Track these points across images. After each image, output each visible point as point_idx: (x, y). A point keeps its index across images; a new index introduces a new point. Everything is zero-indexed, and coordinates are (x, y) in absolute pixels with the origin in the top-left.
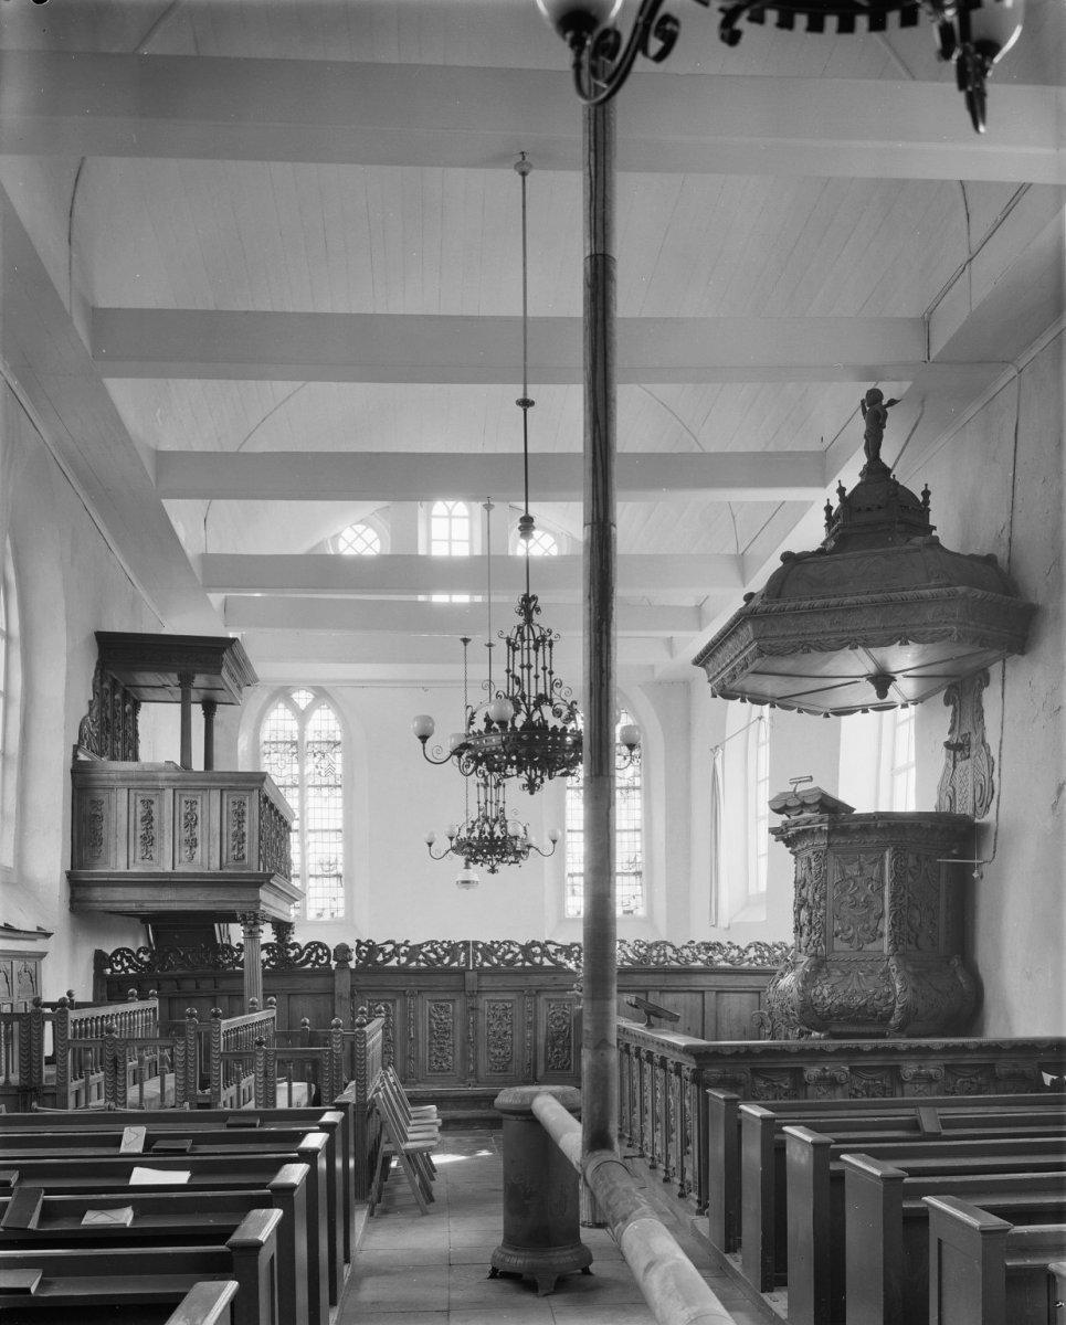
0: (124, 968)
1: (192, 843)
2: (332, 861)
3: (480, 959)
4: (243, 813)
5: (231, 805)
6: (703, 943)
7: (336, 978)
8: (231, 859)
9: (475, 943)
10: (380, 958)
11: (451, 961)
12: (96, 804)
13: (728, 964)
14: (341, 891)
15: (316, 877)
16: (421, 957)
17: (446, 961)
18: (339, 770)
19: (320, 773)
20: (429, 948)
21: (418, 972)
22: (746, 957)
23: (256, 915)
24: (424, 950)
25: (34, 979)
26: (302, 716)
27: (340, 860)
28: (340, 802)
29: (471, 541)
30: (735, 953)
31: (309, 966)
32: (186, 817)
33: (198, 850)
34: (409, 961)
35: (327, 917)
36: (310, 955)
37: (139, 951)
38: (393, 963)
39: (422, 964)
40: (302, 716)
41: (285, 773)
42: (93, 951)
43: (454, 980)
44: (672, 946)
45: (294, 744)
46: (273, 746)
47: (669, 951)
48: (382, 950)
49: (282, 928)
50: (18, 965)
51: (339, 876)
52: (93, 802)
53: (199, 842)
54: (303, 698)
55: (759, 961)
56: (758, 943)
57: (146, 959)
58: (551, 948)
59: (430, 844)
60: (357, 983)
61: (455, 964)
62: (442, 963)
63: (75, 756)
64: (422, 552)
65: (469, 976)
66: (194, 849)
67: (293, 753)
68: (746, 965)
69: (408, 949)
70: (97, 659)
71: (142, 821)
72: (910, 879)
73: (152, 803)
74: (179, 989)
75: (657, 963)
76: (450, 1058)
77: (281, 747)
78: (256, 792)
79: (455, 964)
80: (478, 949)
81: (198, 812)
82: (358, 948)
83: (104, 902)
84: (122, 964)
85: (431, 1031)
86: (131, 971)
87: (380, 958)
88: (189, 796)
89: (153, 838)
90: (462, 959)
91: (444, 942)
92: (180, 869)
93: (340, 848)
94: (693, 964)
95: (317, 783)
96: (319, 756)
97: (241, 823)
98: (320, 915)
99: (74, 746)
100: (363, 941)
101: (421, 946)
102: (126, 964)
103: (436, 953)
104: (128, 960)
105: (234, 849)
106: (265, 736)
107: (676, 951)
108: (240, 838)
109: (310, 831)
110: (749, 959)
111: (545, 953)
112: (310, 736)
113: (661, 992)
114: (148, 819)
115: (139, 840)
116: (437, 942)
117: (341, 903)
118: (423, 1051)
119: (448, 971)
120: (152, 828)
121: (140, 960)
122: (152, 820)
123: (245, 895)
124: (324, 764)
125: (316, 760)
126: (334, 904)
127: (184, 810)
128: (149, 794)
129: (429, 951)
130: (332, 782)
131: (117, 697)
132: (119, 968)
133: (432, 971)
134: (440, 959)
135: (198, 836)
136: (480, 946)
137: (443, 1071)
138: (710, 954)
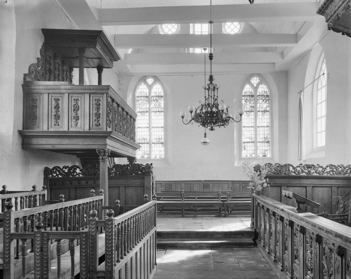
0: (57, 175)
1: (77, 118)
2: (160, 138)
4: (99, 105)
5: (94, 101)
6: (306, 165)
7: (145, 179)
8: (94, 125)
12: (35, 100)
13: (317, 174)
14: (163, 149)
15: (155, 143)
18: (162, 106)
19: (156, 107)
22: (325, 171)
23: (105, 151)
26: (150, 87)
27: (163, 137)
28: (163, 117)
30: (320, 169)
32: (74, 107)
33: (79, 121)
35: (158, 157)
37: (63, 167)
40: (150, 87)
41: (144, 107)
42: (44, 168)
44: (292, 166)
45: (147, 97)
46: (140, 98)
47: (291, 168)
49: (131, 159)
51: (162, 143)
52: (33, 100)
53: (80, 118)
54: (150, 81)
55: (331, 173)
56: (331, 165)
57: (66, 171)
59: (183, 117)
63: (25, 79)
64: (191, 32)
66: (77, 121)
67: (147, 100)
68: (325, 174)
70: (43, 41)
73: (59, 100)
75: (285, 174)
77: (143, 98)
78: (105, 95)
81: (79, 104)
83: (37, 145)
84: (56, 173)
86: (60, 176)
88: (75, 97)
89: (59, 116)
92: (71, 130)
93: (163, 133)
94: (302, 174)
95: (155, 111)
96: (156, 101)
97: (98, 109)
98: (156, 157)
99: (25, 75)
102: (58, 173)
104: (59, 171)
106: (137, 94)
107: (294, 168)
108: (98, 116)
109: (152, 127)
110: (327, 172)
112: (153, 94)
113: (288, 186)
114: (57, 107)
115: (53, 117)
117: (163, 153)
120: (59, 111)
121: (64, 171)
122: (59, 108)
123: (100, 142)
124: (157, 104)
125: (155, 102)
126: (161, 153)
127: (73, 103)
128: (58, 96)
130: (160, 110)
131: (65, 68)
132: (55, 175)
135: (79, 115)
138: (309, 170)
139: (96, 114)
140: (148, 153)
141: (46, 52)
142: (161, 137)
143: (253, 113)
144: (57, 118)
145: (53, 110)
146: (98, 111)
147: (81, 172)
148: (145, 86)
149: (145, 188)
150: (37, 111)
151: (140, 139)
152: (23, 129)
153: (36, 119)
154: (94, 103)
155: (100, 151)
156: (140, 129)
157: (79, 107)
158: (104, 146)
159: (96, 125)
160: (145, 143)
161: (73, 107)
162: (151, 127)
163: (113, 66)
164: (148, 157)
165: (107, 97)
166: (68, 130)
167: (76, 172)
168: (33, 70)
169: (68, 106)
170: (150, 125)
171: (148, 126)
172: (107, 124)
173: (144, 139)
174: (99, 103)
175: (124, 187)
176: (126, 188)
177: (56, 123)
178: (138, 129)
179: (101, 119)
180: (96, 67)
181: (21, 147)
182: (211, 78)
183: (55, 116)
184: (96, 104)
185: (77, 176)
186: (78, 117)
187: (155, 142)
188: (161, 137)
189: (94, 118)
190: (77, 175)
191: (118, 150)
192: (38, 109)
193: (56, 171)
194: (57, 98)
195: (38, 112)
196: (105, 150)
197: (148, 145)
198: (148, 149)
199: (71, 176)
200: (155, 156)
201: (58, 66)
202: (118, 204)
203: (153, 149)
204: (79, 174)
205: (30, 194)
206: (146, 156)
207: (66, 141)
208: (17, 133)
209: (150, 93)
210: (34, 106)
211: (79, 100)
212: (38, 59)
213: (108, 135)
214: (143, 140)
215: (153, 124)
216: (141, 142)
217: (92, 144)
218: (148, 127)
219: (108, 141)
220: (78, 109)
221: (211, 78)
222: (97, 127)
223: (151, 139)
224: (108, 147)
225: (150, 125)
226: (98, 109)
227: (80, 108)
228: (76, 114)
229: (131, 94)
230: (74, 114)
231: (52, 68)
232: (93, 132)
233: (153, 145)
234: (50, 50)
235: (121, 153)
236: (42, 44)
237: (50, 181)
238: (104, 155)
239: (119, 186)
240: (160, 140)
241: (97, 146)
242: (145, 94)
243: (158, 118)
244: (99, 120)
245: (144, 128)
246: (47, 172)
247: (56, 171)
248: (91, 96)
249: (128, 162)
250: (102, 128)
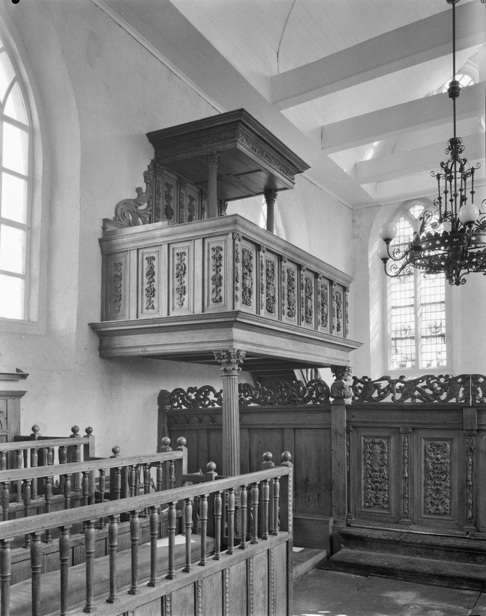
1: (182, 291)
3: (481, 395)
4: (220, 258)
5: (211, 251)
7: (333, 414)
8: (211, 302)
9: (476, 377)
10: (375, 395)
11: (450, 397)
12: (118, 265)
14: (444, 347)
15: (427, 337)
16: (417, 393)
17: (444, 397)
20: (424, 384)
21: (413, 409)
23: (229, 354)
24: (419, 386)
27: (444, 324)
31: (310, 403)
32: (177, 269)
33: (186, 297)
34: (405, 396)
35: (434, 365)
36: (311, 393)
38: (388, 399)
39: (418, 401)
42: (158, 391)
48: (377, 387)
51: (442, 336)
53: (186, 290)
57: (193, 397)
60: (353, 419)
61: (453, 400)
62: (439, 399)
63: (104, 228)
65: (467, 412)
66: (183, 296)
69: (403, 385)
70: (152, 156)
71: (147, 275)
73: (154, 258)
74: (213, 422)
76: (448, 501)
78: (230, 236)
79: (453, 400)
80: (478, 384)
81: (186, 262)
82: (355, 384)
83: (120, 348)
84: (178, 402)
85: (426, 468)
86: (184, 407)
87: (375, 395)
89: (154, 290)
90: (461, 395)
91: (441, 376)
92: (172, 314)
93: (443, 315)
97: (218, 267)
98: (429, 365)
99: (105, 221)
100: (359, 377)
101: (416, 382)
103: (432, 389)
104: (182, 398)
105: (213, 291)
108: (218, 281)
109: (422, 304)
114: (151, 273)
115: (145, 292)
116: (433, 377)
117: (444, 356)
118: (419, 492)
119: (445, 408)
120: (154, 281)
121: (189, 398)
122: (154, 274)
126: (439, 356)
127: (176, 262)
128: (151, 252)
129: (425, 387)
133: (429, 407)
134: (436, 395)
135: (185, 284)
136: (481, 380)
137: (439, 514)
139: (214, 279)
140: (414, 357)
141: (156, 177)
142: (441, 324)
144: (151, 294)
145: (146, 280)
146: (217, 272)
147: (216, 399)
148: (407, 223)
149: (333, 433)
150: (121, 286)
151: (396, 331)
152: (102, 320)
153: (120, 299)
154: (211, 255)
155: (220, 354)
156: (398, 310)
157: (185, 268)
158: (227, 344)
159: (214, 302)
160: (406, 338)
161: (175, 269)
162: (418, 304)
163: (294, 184)
164: (413, 366)
165: (234, 240)
166: (168, 314)
167: (208, 399)
168: (123, 211)
169: (167, 269)
170: (416, 301)
171: (412, 303)
172: (234, 298)
173: (406, 330)
174: (220, 255)
175: (292, 431)
176: (297, 432)
177: (150, 305)
178: (393, 311)
179: (222, 288)
180: (263, 191)
181: (98, 354)
183: (148, 291)
184: (214, 258)
185: (210, 406)
186: (185, 287)
187: (428, 334)
188: (441, 324)
189: (212, 287)
190: (209, 404)
191: (280, 351)
192: (122, 280)
193: (177, 397)
194: (152, 255)
195: (122, 288)
196: (230, 351)
197: (413, 342)
198: (414, 350)
199: (200, 407)
200: (428, 362)
201: (188, 201)
202: (213, 472)
203: (424, 349)
204: (212, 403)
205: (40, 445)
206: (409, 365)
207: (164, 338)
208: (86, 329)
210: (116, 276)
211: (185, 255)
212: (139, 190)
213: (232, 319)
214: (403, 332)
215: (423, 298)
216: (400, 337)
217: (206, 340)
218: (413, 306)
219: (237, 333)
220: (184, 273)
222: (217, 305)
223: (419, 328)
224: (237, 346)
225: (416, 301)
226: (217, 267)
227: (187, 271)
228: (181, 283)
229: (377, 242)
230: (177, 284)
231: (173, 205)
232: (211, 316)
233: (424, 341)
234: (165, 172)
235: (303, 359)
236: (149, 163)
237: (168, 416)
238: (229, 363)
239: (282, 427)
240: (438, 330)
241: (215, 345)
242: (407, 238)
243: (433, 285)
244: (220, 290)
245: (405, 307)
246: (164, 399)
247: (177, 397)
248: (207, 241)
249: (333, 376)
250: (225, 306)
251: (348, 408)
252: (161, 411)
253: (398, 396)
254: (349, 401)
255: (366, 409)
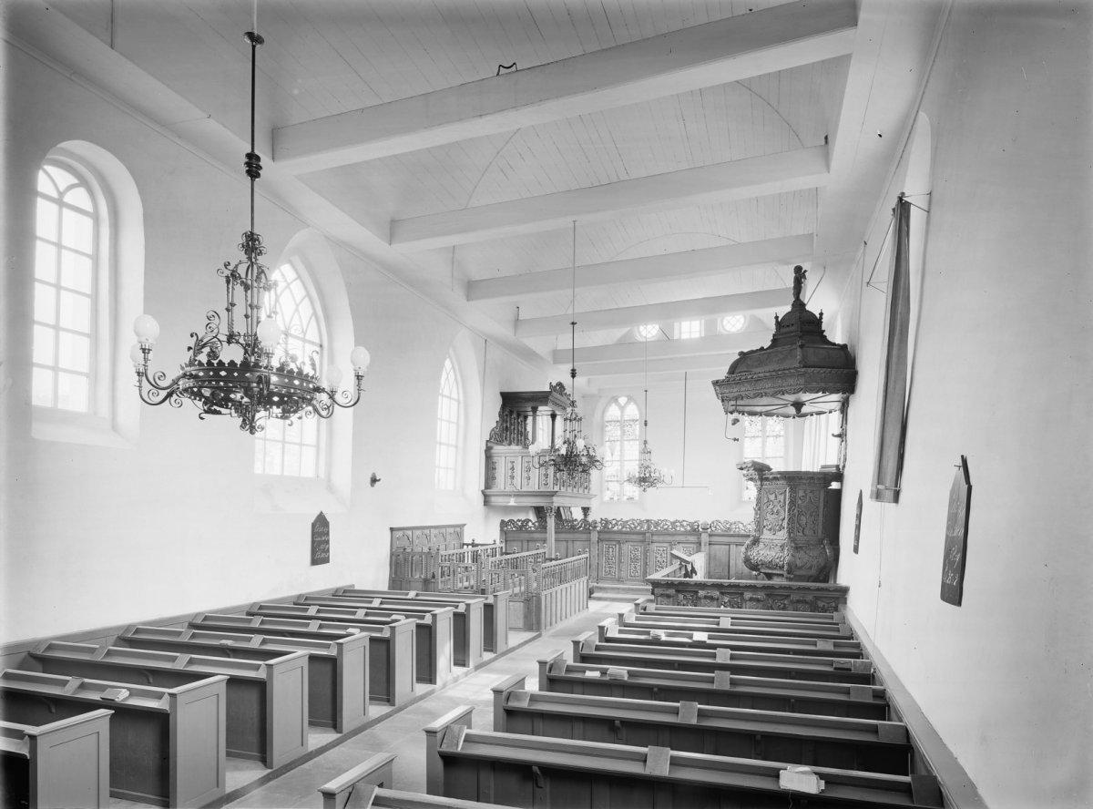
18: (637, 432)
21: (626, 533)
25: (460, 535)
26: (622, 408)
29: (700, 331)
38: (616, 528)
40: (622, 408)
43: (640, 537)
50: (452, 530)
54: (623, 400)
58: (685, 524)
65: (647, 535)
72: (800, 502)
101: (627, 522)
111: (683, 526)
114: (513, 468)
123: (548, 500)
128: (513, 459)
143: (760, 439)
145: (510, 471)
182: (645, 442)
209: (622, 416)
221: (645, 442)
246: (503, 524)
251: (598, 532)
252: (502, 530)
253: (620, 527)
254: (598, 529)
255: (605, 532)
